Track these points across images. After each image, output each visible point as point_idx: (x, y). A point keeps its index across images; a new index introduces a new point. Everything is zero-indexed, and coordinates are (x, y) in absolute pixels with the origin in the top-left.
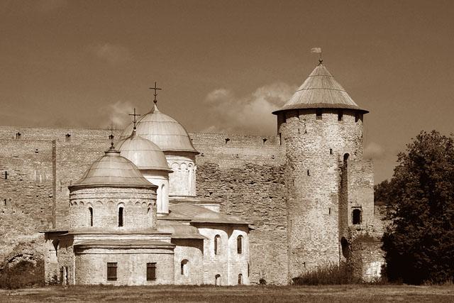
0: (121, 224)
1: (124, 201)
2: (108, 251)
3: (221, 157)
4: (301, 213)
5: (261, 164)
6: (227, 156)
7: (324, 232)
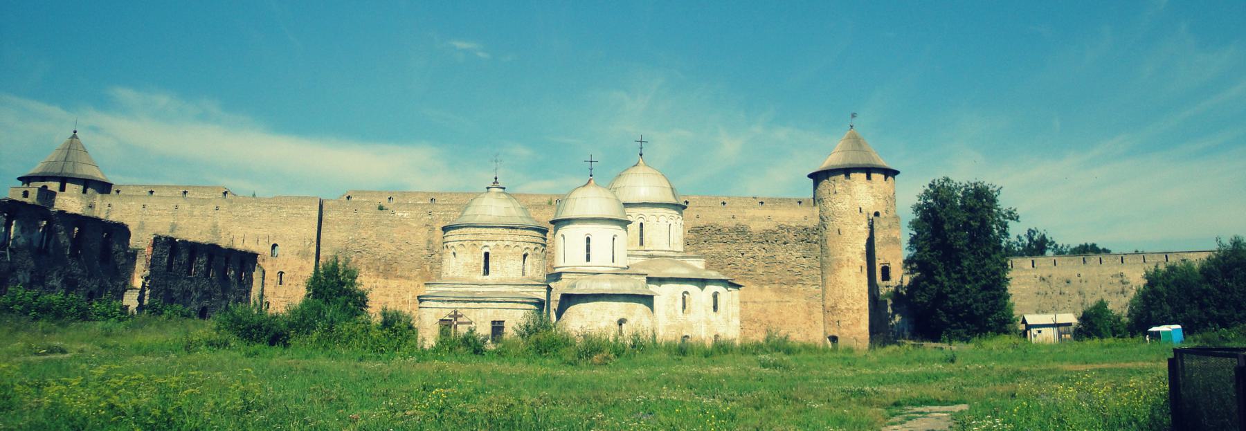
0: (486, 272)
1: (491, 244)
2: (440, 305)
3: (753, 219)
4: (833, 272)
5: (794, 225)
6: (759, 218)
7: (855, 291)
